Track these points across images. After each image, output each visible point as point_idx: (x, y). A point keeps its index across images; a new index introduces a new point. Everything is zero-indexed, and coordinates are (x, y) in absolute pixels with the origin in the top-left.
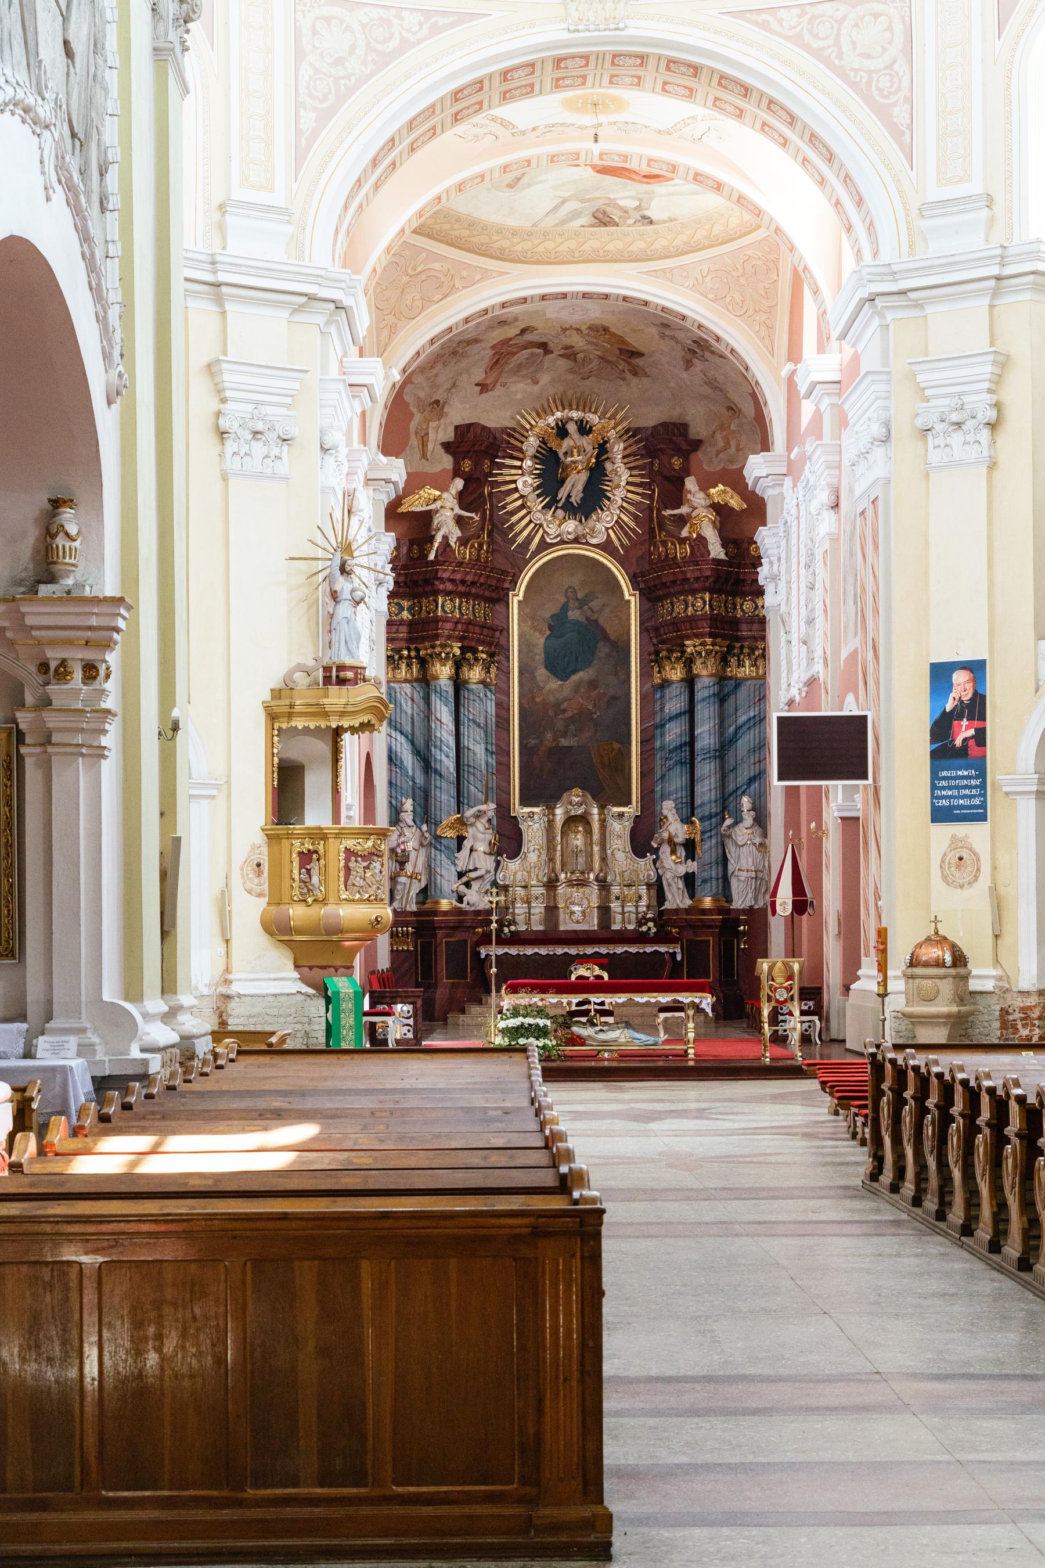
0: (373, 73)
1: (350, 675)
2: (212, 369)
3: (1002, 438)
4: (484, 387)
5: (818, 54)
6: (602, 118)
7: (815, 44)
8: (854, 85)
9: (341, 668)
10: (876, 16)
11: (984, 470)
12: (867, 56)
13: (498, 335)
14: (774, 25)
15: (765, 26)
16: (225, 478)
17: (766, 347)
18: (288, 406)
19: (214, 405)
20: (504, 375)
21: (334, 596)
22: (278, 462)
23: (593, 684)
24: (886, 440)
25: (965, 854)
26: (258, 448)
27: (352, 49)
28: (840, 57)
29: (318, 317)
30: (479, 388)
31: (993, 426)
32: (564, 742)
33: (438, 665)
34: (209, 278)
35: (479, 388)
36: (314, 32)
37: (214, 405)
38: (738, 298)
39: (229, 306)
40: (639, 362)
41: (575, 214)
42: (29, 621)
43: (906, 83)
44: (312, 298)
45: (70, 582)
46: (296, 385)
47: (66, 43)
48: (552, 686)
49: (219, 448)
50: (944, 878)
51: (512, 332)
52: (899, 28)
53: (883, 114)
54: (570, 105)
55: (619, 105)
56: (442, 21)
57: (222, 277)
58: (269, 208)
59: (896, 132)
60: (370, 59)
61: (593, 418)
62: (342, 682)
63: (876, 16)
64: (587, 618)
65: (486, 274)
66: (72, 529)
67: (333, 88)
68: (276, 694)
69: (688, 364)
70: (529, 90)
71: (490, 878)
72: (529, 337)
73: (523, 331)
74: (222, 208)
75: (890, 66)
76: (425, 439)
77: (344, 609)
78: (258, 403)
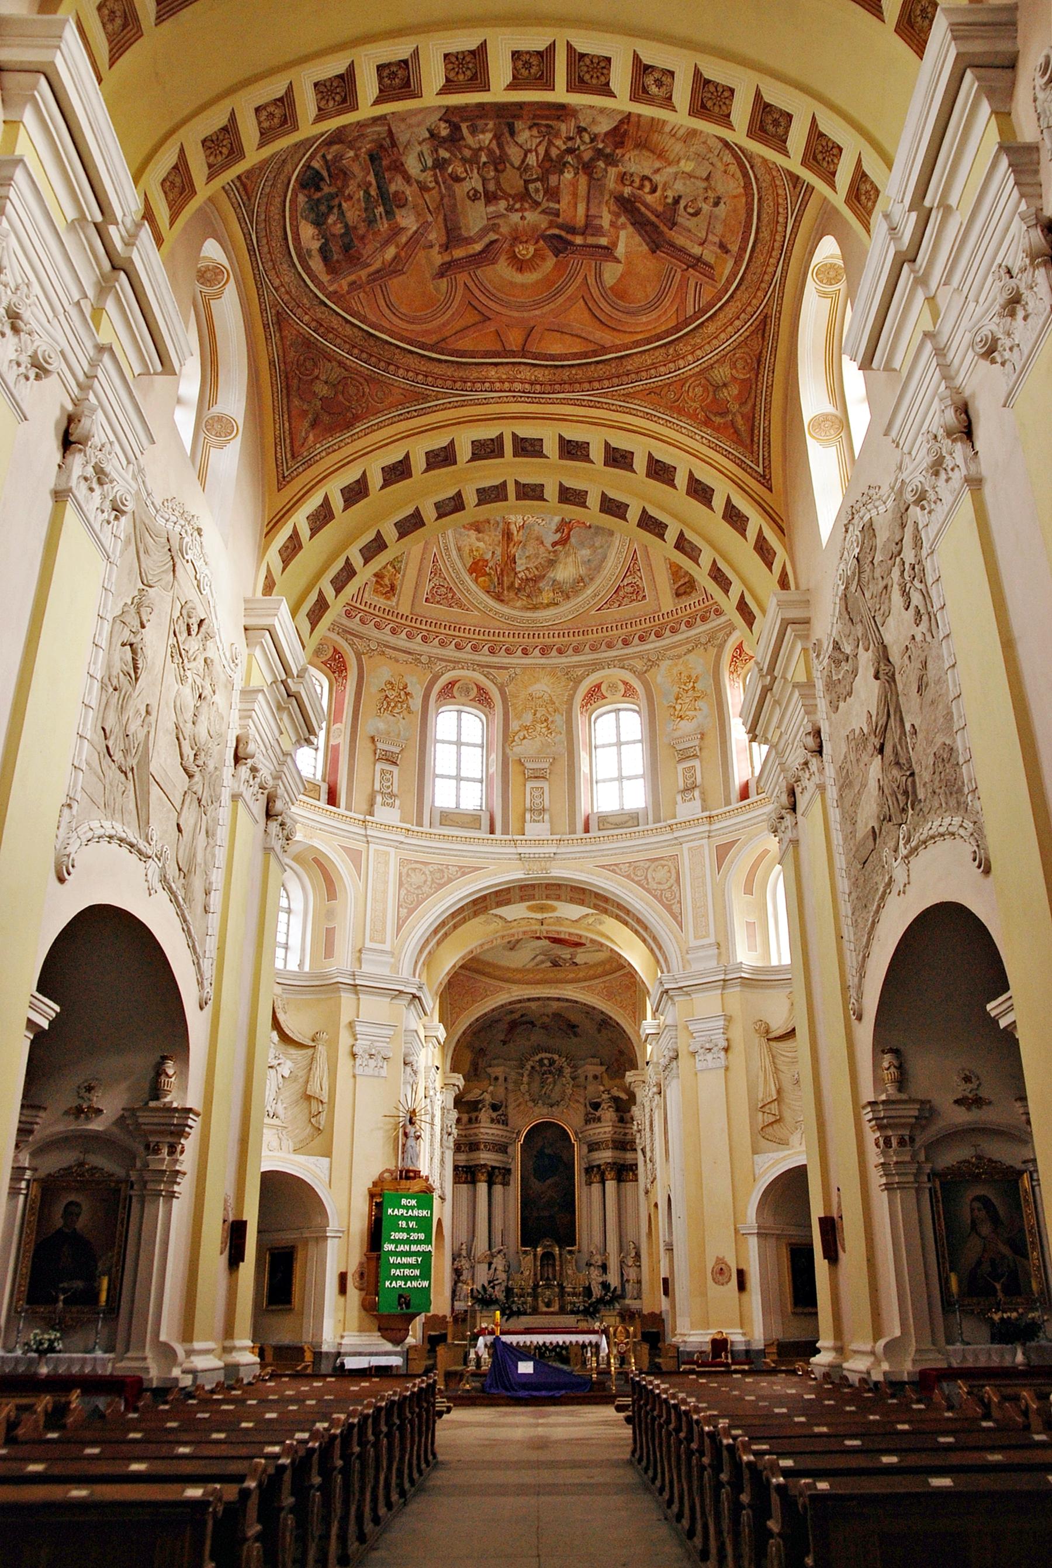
1: (412, 1174)
2: (351, 1025)
3: (730, 1056)
5: (638, 883)
6: (545, 915)
7: (636, 879)
8: (655, 896)
9: (408, 1171)
10: (663, 866)
11: (723, 1070)
12: (660, 883)
13: (509, 1018)
14: (618, 871)
15: (613, 871)
16: (354, 1076)
18: (388, 1043)
19: (351, 1041)
21: (406, 1135)
24: (676, 1057)
25: (723, 1266)
26: (372, 1063)
27: (425, 882)
28: (648, 884)
29: (404, 1002)
31: (726, 1050)
34: (352, 982)
36: (408, 875)
37: (351, 1041)
38: (619, 999)
39: (361, 996)
41: (543, 962)
42: (141, 1120)
43: (678, 895)
44: (401, 992)
45: (167, 1099)
46: (392, 1033)
47: (178, 825)
48: (536, 1185)
49: (352, 1063)
50: (714, 1279)
51: (516, 1016)
52: (673, 871)
53: (669, 908)
54: (530, 908)
55: (553, 909)
56: (467, 870)
57: (358, 982)
58: (382, 951)
59: (675, 917)
61: (556, 1057)
62: (408, 1178)
63: (663, 866)
65: (502, 989)
66: (170, 1072)
68: (375, 1184)
69: (599, 1031)
70: (508, 902)
71: (504, 1284)
72: (524, 1019)
73: (522, 1016)
74: (360, 951)
75: (670, 888)
77: (411, 1142)
78: (373, 1041)
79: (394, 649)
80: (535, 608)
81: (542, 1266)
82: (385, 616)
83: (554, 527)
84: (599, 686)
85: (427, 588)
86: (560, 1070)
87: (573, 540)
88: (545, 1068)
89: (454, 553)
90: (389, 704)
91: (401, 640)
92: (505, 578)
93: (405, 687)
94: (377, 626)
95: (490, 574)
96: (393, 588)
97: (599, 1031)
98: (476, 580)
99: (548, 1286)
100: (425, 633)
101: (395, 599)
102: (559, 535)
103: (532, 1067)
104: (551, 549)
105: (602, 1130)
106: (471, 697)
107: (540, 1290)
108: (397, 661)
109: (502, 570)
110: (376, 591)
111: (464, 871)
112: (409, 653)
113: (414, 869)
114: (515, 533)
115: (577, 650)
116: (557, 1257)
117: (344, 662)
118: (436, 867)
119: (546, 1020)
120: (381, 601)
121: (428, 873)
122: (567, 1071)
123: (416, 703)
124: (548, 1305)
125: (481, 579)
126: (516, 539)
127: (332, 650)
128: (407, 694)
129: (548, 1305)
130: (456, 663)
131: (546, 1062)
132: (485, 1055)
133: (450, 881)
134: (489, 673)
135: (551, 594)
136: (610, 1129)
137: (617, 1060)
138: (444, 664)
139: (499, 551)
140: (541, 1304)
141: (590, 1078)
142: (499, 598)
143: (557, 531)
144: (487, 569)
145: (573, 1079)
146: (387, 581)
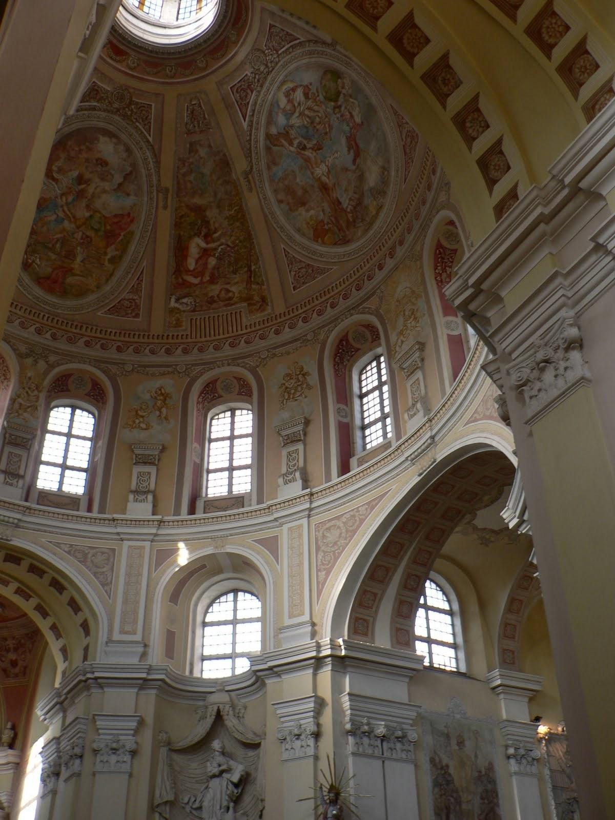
0: (350, 541)
15: (474, 421)
22: (308, 748)
56: (374, 503)
60: (348, 536)
67: (333, 557)
79: (283, 345)
80: (370, 225)
82: (266, 325)
83: (345, 149)
84: (439, 246)
85: (291, 279)
87: (361, 146)
89: (298, 237)
90: (289, 393)
91: (288, 334)
92: (341, 222)
93: (302, 369)
94: (262, 338)
95: (330, 229)
96: (264, 300)
98: (323, 243)
100: (303, 315)
101: (269, 307)
102: (352, 151)
104: (354, 167)
106: (370, 339)
108: (288, 353)
109: (336, 218)
110: (251, 312)
111: (371, 505)
112: (296, 340)
113: (329, 529)
114: (327, 181)
115: (409, 231)
117: (248, 384)
118: (348, 516)
120: (258, 317)
121: (342, 525)
123: (313, 379)
125: (326, 238)
126: (330, 184)
127: (235, 381)
128: (304, 375)
130: (335, 321)
133: (362, 521)
134: (364, 308)
135: (375, 203)
138: (326, 328)
139: (326, 205)
142: (346, 241)
143: (349, 150)
144: (326, 227)
146: (257, 298)
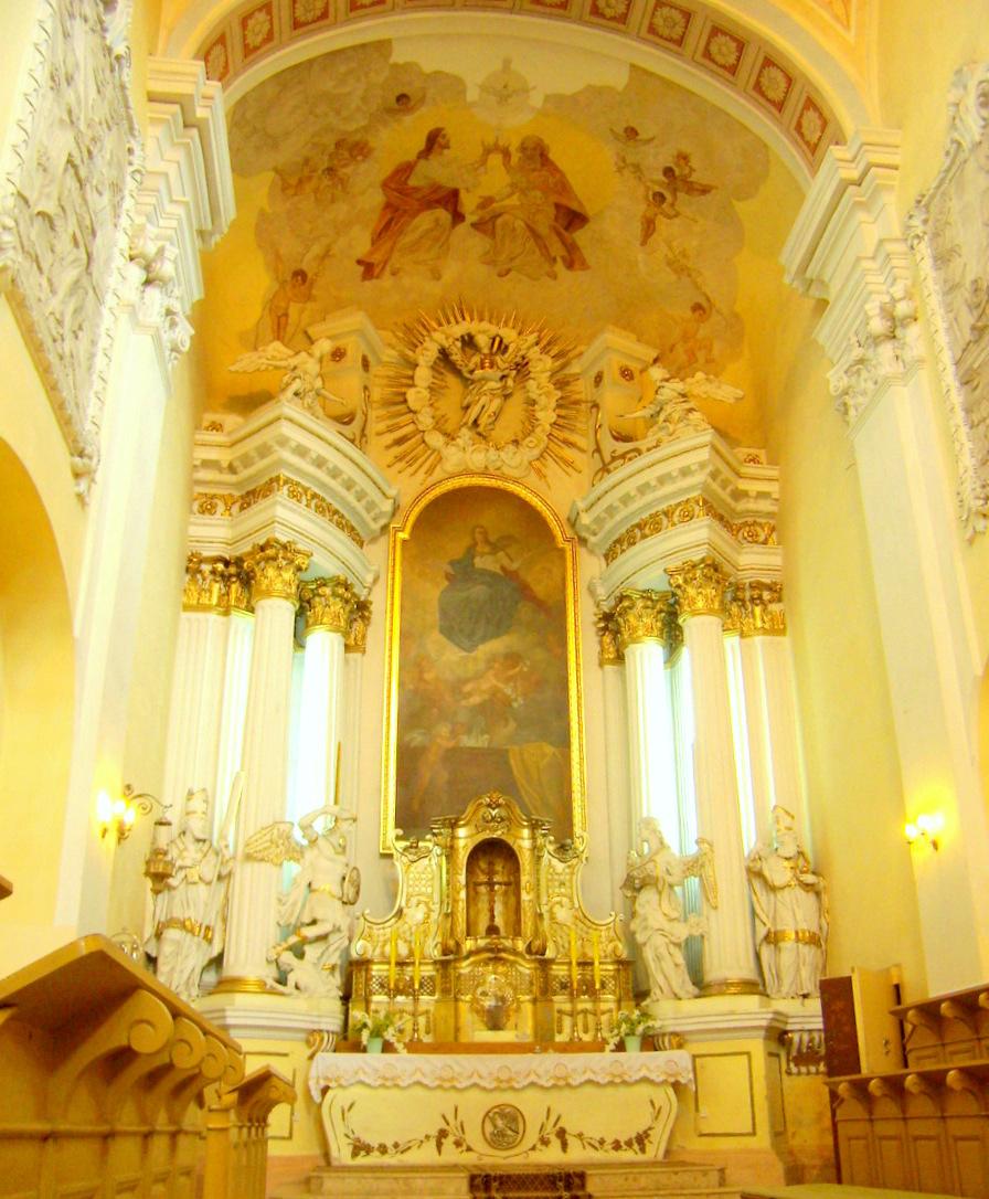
4: (369, 270)
17: (836, 18)
20: (396, 255)
23: (512, 658)
30: (361, 269)
32: (468, 742)
33: (271, 572)
35: (361, 269)
40: (581, 237)
48: (448, 658)
61: (509, 335)
64: (503, 568)
71: (338, 942)
73: (434, 141)
76: (283, 320)
81: (472, 886)
86: (522, 367)
88: (476, 359)
97: (649, 227)
99: (495, 955)
103: (444, 354)
105: (673, 466)
107: (465, 968)
116: (525, 859)
119: (495, 180)
122: (542, 366)
124: (495, 1020)
129: (495, 1020)
131: (482, 341)
132: (309, 297)
136: (704, 454)
137: (685, 337)
140: (467, 1016)
141: (611, 375)
145: (561, 384)
